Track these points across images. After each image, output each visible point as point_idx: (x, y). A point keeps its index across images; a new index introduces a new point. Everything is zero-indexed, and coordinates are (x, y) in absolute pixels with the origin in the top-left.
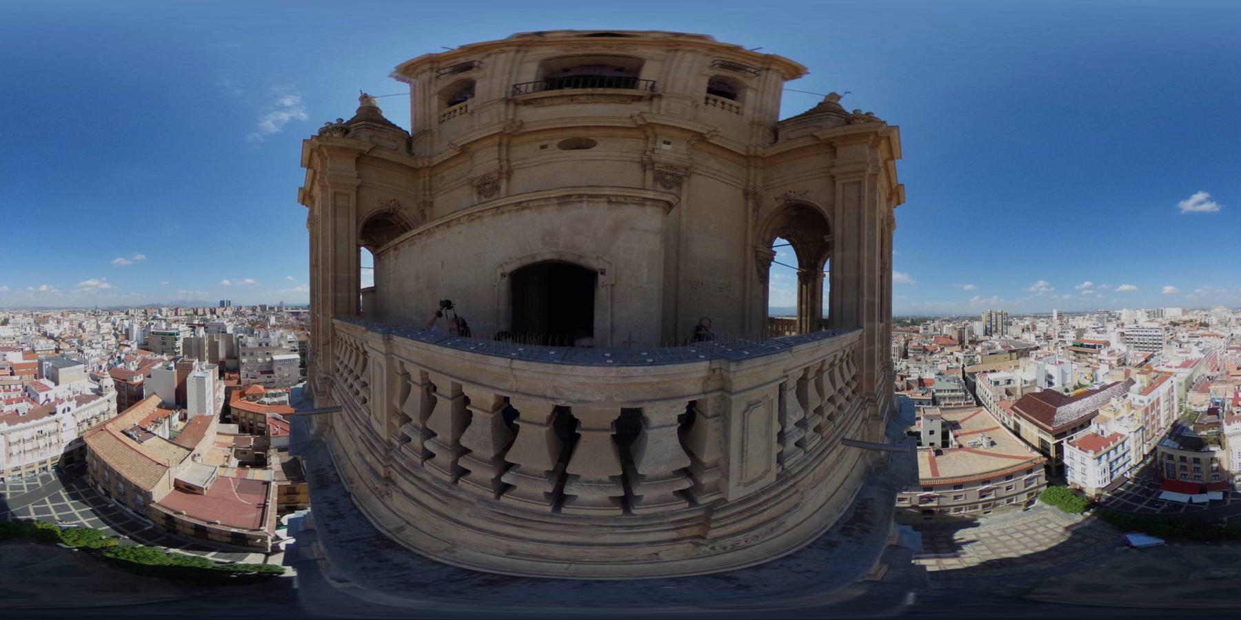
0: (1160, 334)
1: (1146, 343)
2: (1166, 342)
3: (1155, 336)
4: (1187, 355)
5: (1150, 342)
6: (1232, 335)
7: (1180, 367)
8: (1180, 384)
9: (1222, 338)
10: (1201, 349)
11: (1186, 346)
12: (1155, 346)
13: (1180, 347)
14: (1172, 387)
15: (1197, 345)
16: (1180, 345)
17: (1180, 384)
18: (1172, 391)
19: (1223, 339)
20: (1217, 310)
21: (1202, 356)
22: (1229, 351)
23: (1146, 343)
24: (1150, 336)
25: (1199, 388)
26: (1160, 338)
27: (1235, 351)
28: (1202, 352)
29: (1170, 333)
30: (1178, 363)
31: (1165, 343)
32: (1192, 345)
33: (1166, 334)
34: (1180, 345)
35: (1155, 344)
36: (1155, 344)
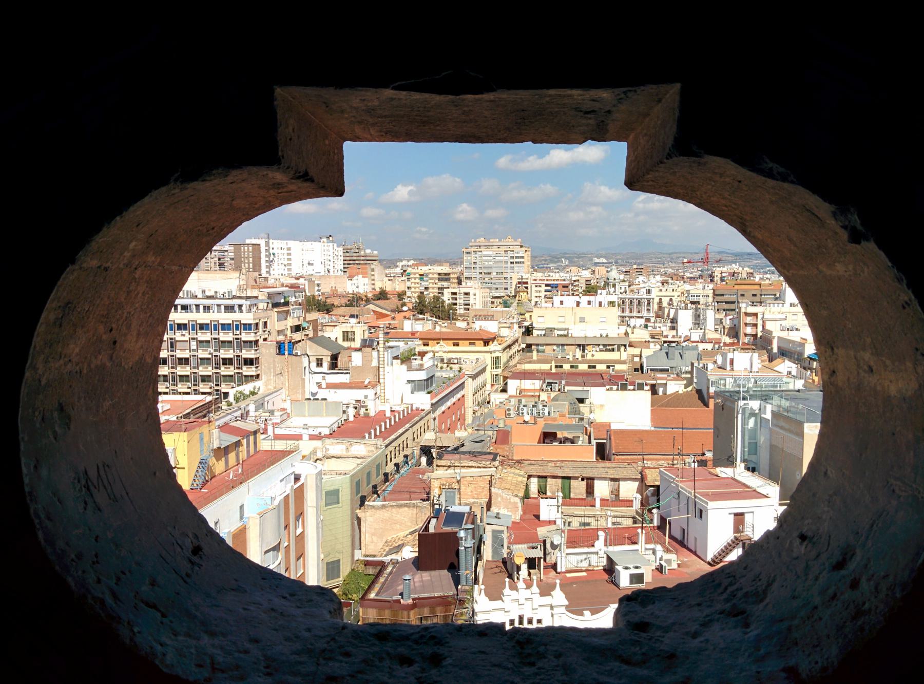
0: (246, 318)
1: (184, 361)
2: (273, 350)
3: (225, 327)
4: (359, 394)
5: (202, 354)
6: (528, 331)
7: (331, 435)
8: (332, 497)
9: (486, 343)
10: (422, 376)
11: (357, 359)
12: (224, 371)
13: (334, 365)
14: (299, 493)
15: (405, 359)
16: (335, 358)
17: (332, 497)
18: (300, 515)
19: (493, 346)
20: (488, 256)
21: (423, 400)
22: (513, 385)
23: (184, 361)
24: (202, 327)
25: (389, 487)
26: (245, 336)
27: (537, 384)
28: (417, 386)
29: (291, 322)
30: (326, 422)
31: (266, 352)
32: (382, 356)
33: (275, 324)
34: (335, 358)
35: (227, 362)
36: (227, 362)
